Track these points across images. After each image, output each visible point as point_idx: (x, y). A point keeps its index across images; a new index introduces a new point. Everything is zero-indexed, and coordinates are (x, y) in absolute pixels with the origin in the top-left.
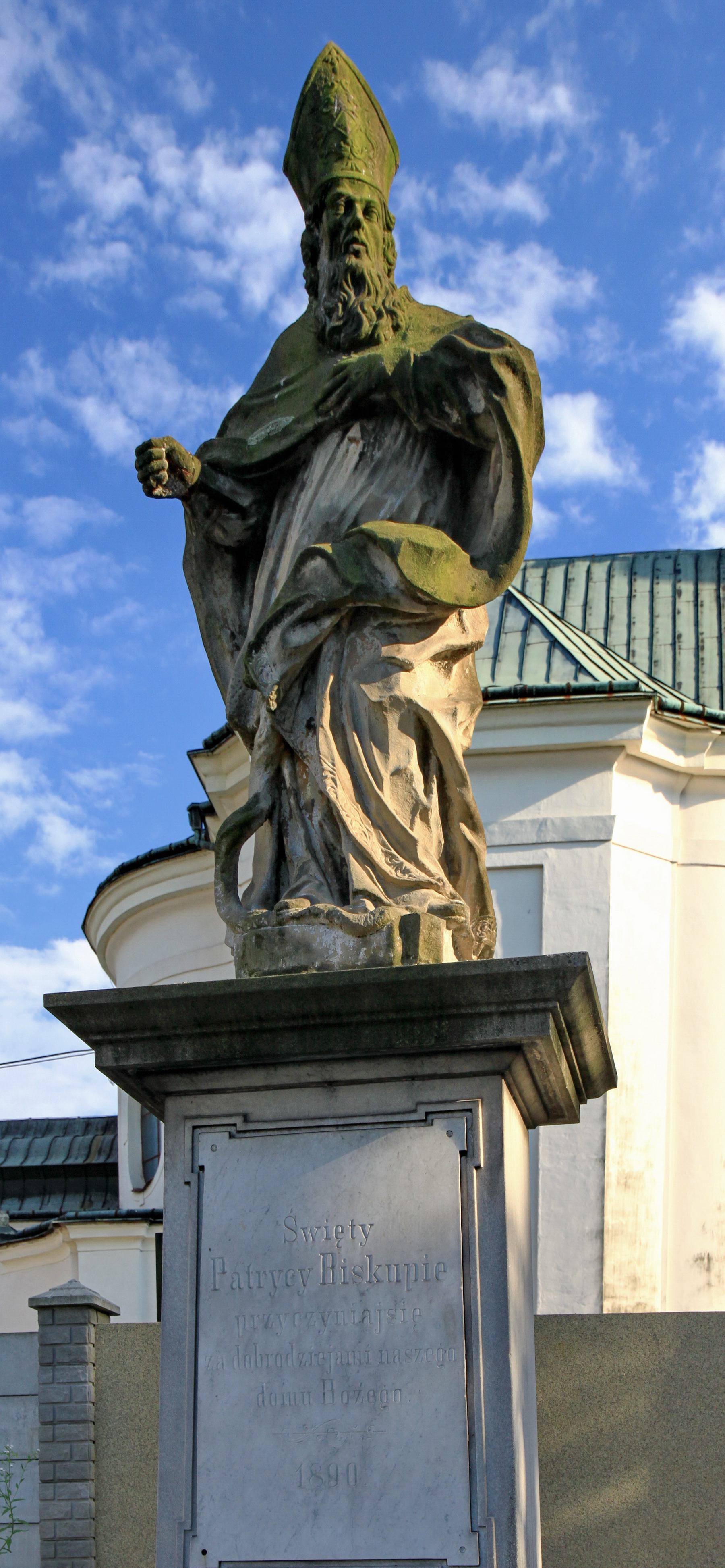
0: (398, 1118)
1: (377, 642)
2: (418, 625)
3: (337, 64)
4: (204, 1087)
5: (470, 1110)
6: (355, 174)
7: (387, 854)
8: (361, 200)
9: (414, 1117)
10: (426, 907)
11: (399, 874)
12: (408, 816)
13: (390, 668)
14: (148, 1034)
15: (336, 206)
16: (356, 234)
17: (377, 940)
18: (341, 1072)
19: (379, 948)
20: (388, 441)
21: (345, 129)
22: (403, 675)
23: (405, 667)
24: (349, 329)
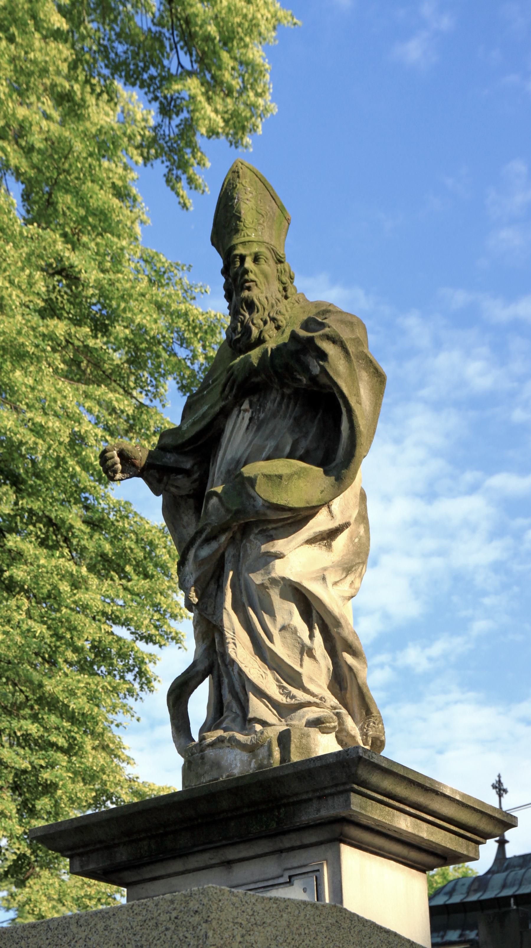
0: (271, 883)
1: (259, 543)
2: (290, 525)
3: (241, 171)
4: (148, 876)
5: (318, 870)
6: (247, 239)
7: (281, 687)
8: (251, 254)
9: (281, 880)
10: (304, 721)
11: (289, 700)
12: (298, 656)
13: (268, 559)
14: (98, 846)
15: (234, 263)
16: (246, 277)
17: (262, 752)
18: (231, 854)
19: (264, 758)
20: (269, 405)
21: (240, 213)
22: (277, 561)
23: (279, 556)
24: (245, 338)
